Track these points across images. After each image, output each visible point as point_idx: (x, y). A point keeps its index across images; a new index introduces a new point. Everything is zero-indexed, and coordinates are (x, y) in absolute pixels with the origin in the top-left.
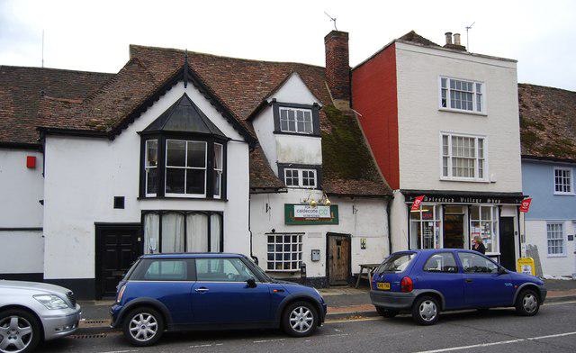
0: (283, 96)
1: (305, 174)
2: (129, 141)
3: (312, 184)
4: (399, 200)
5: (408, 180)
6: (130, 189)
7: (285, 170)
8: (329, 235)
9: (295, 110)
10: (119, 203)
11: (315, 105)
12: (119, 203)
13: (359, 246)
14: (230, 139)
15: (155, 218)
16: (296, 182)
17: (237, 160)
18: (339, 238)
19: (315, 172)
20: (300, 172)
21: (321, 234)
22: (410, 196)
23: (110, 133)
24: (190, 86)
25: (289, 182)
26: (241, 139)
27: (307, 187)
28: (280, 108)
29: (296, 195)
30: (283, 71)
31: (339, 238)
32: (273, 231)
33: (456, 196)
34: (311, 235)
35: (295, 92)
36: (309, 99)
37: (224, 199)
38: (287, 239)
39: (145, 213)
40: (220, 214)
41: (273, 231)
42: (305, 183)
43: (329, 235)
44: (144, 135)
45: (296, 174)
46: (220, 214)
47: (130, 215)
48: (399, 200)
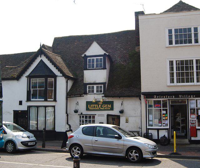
0: (88, 53)
1: (97, 87)
2: (24, 80)
3: (101, 91)
4: (142, 96)
5: (146, 87)
6: (24, 98)
7: (88, 86)
8: (108, 116)
9: (95, 58)
10: (21, 103)
11: (105, 54)
12: (21, 103)
13: (125, 121)
14: (57, 76)
15: (43, 109)
16: (93, 91)
17: (62, 85)
18: (114, 117)
19: (103, 85)
20: (95, 86)
21: (104, 115)
22: (149, 95)
23: (18, 78)
24: (43, 56)
25: (89, 91)
26: (61, 75)
27: (98, 93)
28: (88, 58)
29: (91, 98)
30: (87, 40)
31: (114, 117)
32: (82, 113)
33: (176, 94)
34: (99, 115)
35: (95, 50)
36: (102, 52)
37: (55, 100)
38: (90, 117)
39: (28, 107)
40: (54, 107)
41: (82, 113)
42: (97, 91)
43: (108, 116)
44: (29, 77)
45: (93, 87)
46: (54, 107)
47: (24, 108)
48: (142, 96)
